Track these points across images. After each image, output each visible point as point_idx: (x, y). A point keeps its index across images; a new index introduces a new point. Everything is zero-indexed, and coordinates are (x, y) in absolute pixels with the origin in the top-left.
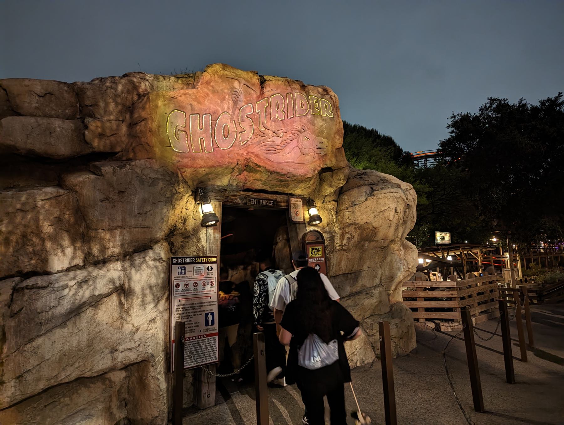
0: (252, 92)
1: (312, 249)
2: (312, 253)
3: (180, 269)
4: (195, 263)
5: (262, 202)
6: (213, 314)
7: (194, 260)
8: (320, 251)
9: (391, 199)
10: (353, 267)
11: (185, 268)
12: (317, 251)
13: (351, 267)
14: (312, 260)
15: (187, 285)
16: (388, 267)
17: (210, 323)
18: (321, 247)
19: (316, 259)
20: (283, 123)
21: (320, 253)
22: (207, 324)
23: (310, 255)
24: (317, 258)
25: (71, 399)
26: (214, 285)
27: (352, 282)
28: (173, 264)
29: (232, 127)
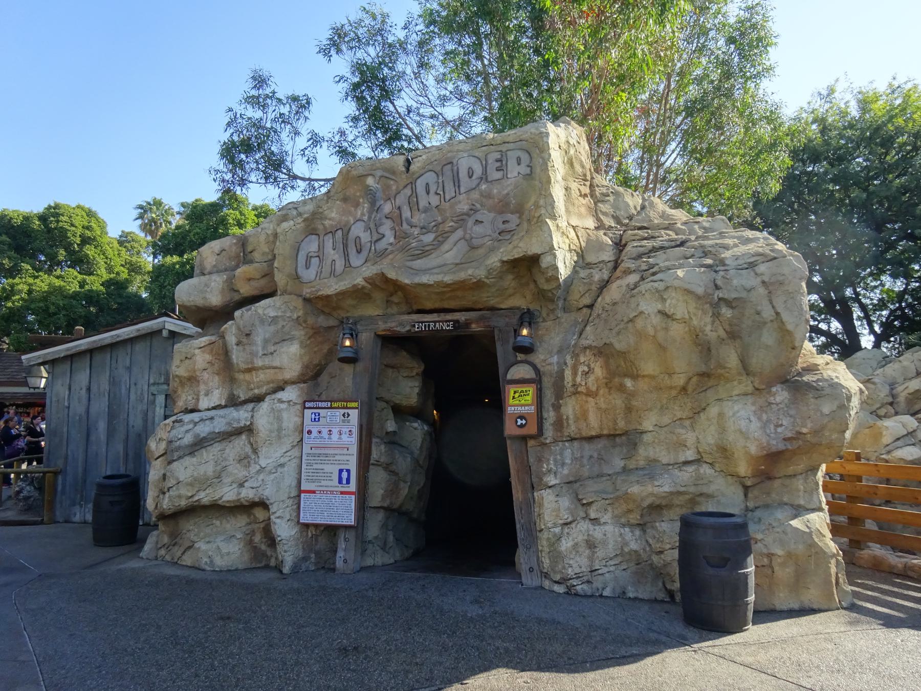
0: (392, 182)
1: (515, 392)
2: (514, 398)
3: (313, 415)
4: (331, 408)
5: (435, 326)
6: (348, 471)
7: (329, 405)
8: (528, 395)
9: (647, 296)
10: (615, 423)
11: (319, 415)
12: (523, 394)
13: (610, 424)
14: (513, 408)
15: (320, 432)
16: (713, 428)
17: (344, 482)
18: (531, 389)
19: (519, 408)
20: (439, 210)
21: (529, 398)
22: (340, 481)
23: (511, 401)
24: (522, 406)
25: (221, 523)
26: (354, 435)
27: (625, 451)
28: (305, 408)
29: (365, 237)
